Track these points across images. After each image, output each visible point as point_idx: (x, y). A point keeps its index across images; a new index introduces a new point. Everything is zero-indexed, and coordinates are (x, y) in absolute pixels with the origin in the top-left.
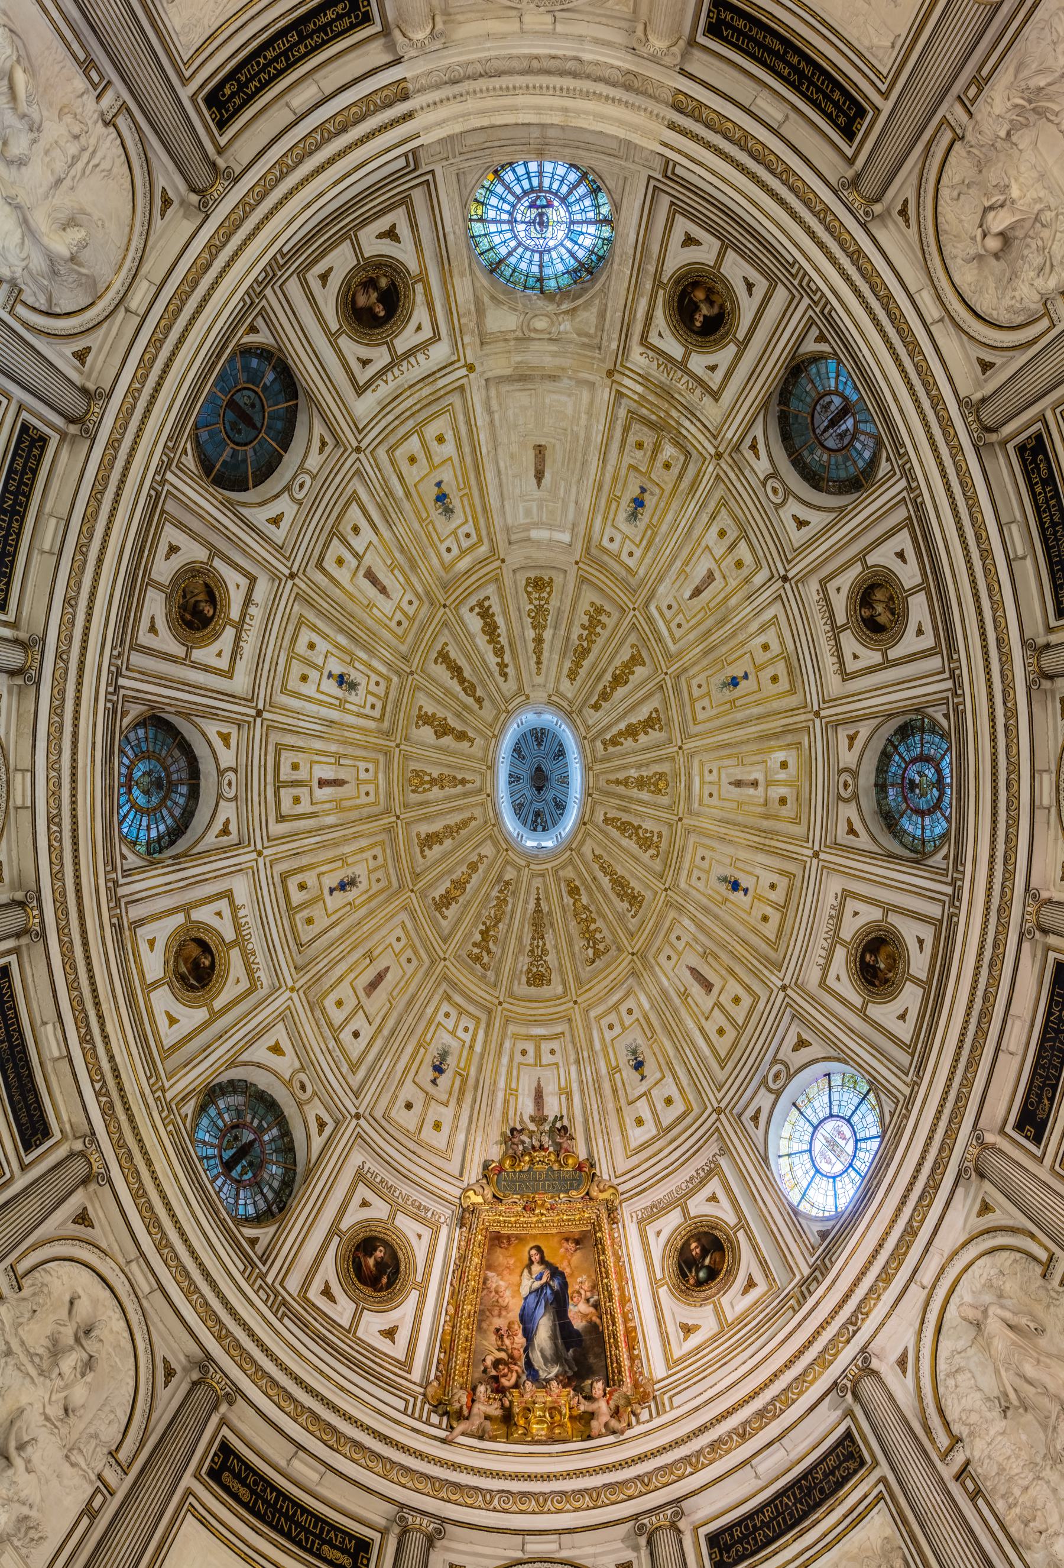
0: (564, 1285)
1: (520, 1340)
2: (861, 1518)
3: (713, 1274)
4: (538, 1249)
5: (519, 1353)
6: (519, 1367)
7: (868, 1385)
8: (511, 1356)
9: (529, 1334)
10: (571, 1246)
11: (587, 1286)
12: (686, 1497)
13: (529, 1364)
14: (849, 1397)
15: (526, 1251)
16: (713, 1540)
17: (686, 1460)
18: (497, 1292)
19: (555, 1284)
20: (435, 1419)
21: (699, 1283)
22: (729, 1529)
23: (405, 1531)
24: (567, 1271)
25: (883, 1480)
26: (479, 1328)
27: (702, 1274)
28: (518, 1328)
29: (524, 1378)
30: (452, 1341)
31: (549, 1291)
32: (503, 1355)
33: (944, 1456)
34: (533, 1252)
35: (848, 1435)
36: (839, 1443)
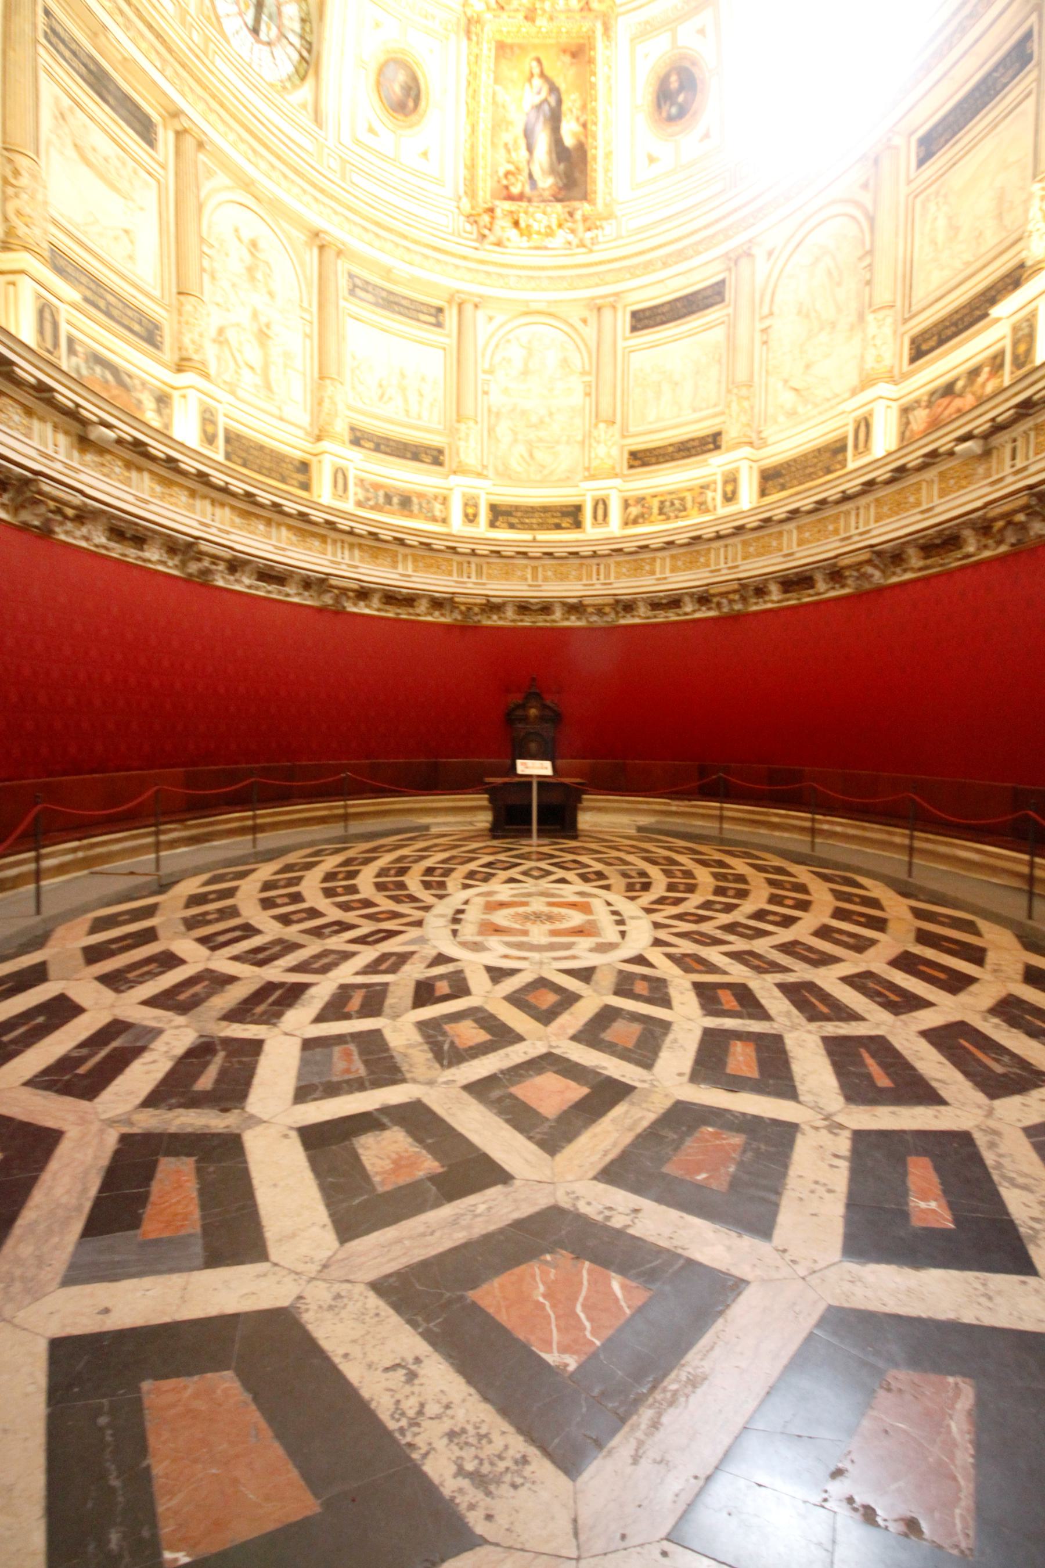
0: (559, 102)
1: (524, 153)
2: (711, 328)
3: (682, 113)
4: (539, 61)
5: (523, 165)
6: (524, 177)
7: (744, 262)
8: (518, 169)
9: (530, 149)
10: (567, 59)
11: (578, 104)
12: (622, 292)
13: (531, 176)
14: (732, 264)
15: (528, 64)
16: (634, 314)
17: (628, 268)
18: (504, 107)
19: (552, 100)
20: (468, 227)
21: (670, 119)
22: (643, 311)
23: (460, 306)
24: (562, 86)
25: (728, 315)
26: (493, 144)
27: (674, 110)
28: (522, 143)
29: (527, 190)
30: (473, 159)
31: (546, 107)
32: (511, 168)
33: (762, 318)
34: (535, 64)
35: (723, 282)
36: (717, 284)
